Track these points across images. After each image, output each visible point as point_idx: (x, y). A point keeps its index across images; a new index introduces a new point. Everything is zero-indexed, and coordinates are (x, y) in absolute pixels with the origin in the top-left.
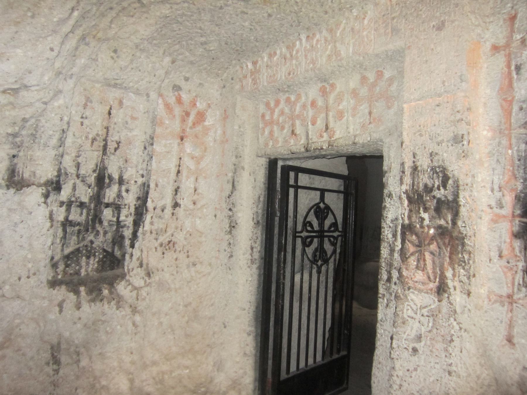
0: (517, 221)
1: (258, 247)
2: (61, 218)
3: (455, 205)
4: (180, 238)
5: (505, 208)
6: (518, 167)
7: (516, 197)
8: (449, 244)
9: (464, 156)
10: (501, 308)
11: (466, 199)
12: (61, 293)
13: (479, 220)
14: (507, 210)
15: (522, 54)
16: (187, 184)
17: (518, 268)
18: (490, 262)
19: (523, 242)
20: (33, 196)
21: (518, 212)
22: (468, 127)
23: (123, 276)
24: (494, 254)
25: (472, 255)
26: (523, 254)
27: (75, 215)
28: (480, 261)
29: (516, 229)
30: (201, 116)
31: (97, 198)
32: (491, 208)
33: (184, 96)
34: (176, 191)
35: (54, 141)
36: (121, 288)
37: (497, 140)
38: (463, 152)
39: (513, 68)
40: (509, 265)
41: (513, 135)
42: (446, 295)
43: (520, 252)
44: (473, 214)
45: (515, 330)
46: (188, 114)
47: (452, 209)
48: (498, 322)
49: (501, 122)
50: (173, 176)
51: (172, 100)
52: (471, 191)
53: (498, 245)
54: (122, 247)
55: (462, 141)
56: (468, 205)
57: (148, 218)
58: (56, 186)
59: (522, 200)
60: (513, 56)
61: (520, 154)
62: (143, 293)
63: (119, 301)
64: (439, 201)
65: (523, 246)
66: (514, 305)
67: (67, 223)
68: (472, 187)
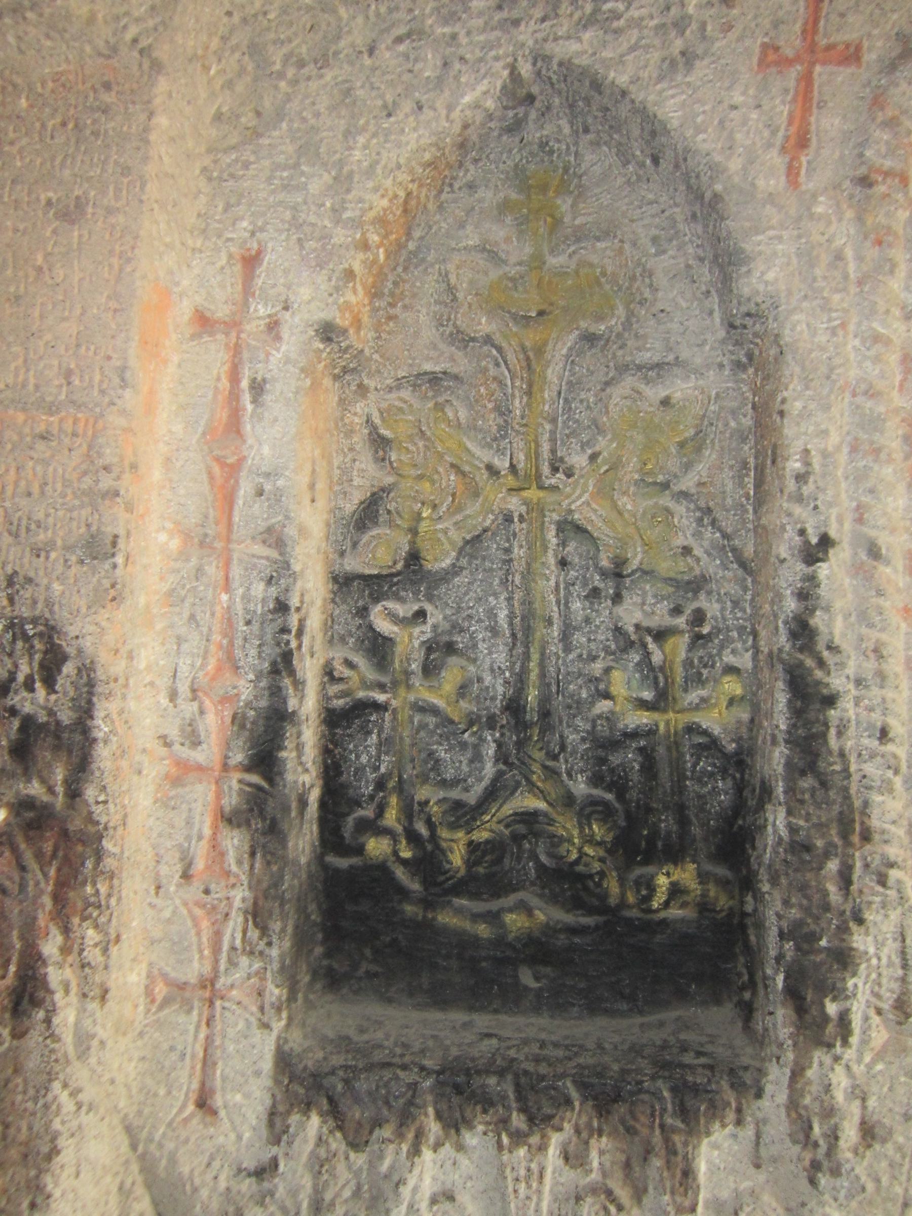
0: (234, 780)
3: (78, 737)
5: (204, 746)
6: (245, 639)
7: (234, 718)
8: (54, 856)
9: (114, 599)
10: (182, 1018)
11: (113, 722)
13: (135, 778)
14: (207, 754)
15: (268, 354)
17: (230, 906)
18: (157, 893)
19: (248, 837)
21: (238, 757)
22: (128, 515)
24: (171, 871)
25: (116, 882)
26: (246, 866)
28: (132, 895)
29: (231, 801)
32: (168, 745)
37: (194, 561)
38: (113, 586)
39: (245, 384)
40: (208, 899)
41: (235, 556)
42: (41, 1014)
43: (239, 862)
44: (124, 764)
45: (218, 1072)
47: (70, 752)
48: (174, 1056)
49: (206, 517)
52: (124, 697)
53: (180, 845)
55: (113, 555)
56: (115, 739)
59: (248, 726)
60: (246, 355)
61: (252, 607)
64: (28, 723)
65: (246, 848)
66: (218, 1003)
68: (126, 686)
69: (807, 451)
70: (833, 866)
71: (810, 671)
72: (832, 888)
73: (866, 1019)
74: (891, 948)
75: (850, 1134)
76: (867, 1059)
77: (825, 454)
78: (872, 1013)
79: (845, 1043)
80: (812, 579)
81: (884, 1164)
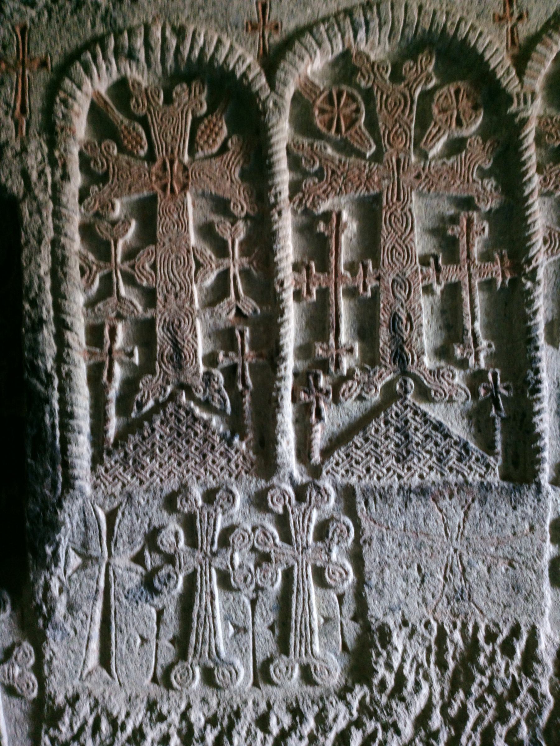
69: (30, 276)
70: (49, 481)
71: (35, 386)
72: (48, 492)
73: (67, 553)
74: (77, 517)
75: (61, 609)
76: (69, 572)
77: (39, 277)
78: (71, 551)
79: (56, 565)
80: (36, 341)
81: (78, 622)
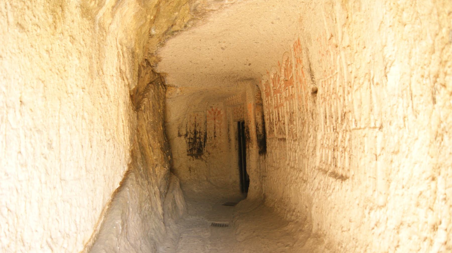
1: (237, 145)
2: (188, 141)
4: (217, 144)
12: (190, 157)
16: (218, 131)
20: (183, 138)
23: (203, 154)
27: (191, 141)
30: (219, 112)
31: (195, 137)
33: (214, 108)
34: (215, 133)
35: (185, 127)
36: (203, 157)
46: (215, 113)
50: (213, 129)
51: (210, 110)
54: (202, 147)
57: (208, 141)
58: (186, 135)
62: (208, 158)
63: (202, 160)
67: (189, 143)
